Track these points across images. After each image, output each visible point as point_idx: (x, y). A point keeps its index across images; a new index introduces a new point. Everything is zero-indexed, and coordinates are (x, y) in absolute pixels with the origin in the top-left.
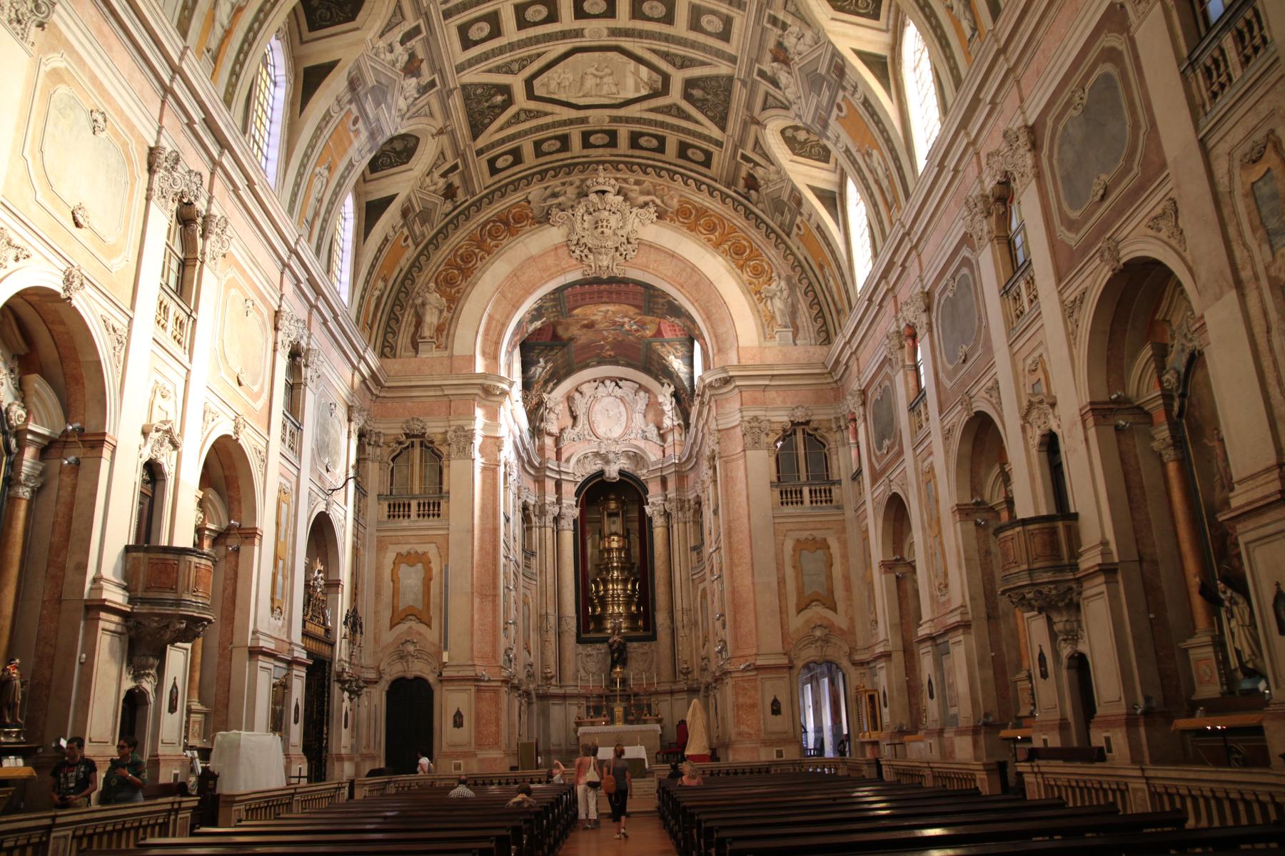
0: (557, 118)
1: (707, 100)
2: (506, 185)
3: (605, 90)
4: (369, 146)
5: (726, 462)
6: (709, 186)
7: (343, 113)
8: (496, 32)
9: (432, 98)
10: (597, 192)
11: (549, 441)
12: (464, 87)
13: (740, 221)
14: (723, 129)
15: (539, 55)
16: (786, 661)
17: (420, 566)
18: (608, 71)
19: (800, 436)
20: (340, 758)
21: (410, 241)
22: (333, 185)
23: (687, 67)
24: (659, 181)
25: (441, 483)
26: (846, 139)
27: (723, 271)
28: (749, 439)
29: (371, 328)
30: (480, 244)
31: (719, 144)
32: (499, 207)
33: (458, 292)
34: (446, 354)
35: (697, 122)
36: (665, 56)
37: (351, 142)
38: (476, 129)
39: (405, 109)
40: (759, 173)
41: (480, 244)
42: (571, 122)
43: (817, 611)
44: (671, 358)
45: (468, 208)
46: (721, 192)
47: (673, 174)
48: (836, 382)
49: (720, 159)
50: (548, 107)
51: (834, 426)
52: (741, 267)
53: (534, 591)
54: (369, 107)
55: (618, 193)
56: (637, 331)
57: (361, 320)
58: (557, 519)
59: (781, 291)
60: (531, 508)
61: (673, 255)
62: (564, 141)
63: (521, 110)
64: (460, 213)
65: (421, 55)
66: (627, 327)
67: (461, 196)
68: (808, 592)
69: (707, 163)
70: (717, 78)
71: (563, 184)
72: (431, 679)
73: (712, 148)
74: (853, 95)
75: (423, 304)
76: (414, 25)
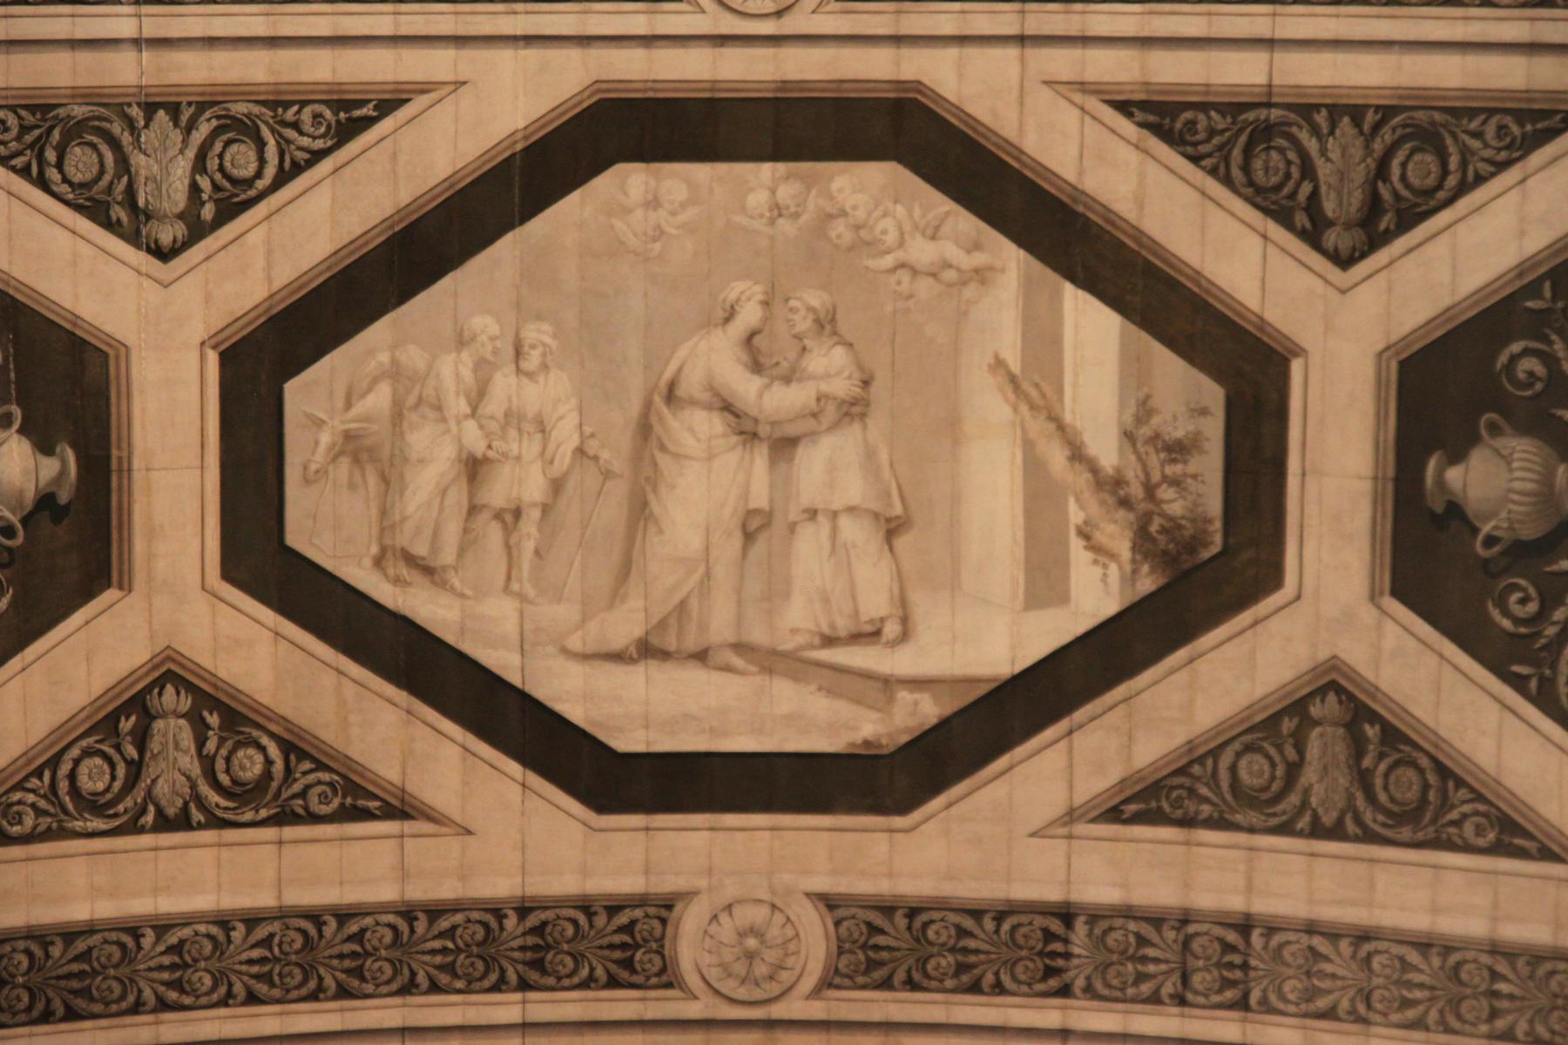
18: (830, 367)
50: (377, 725)
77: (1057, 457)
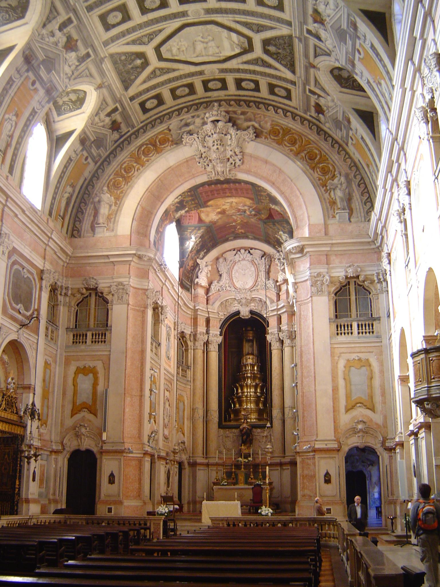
0: (182, 73)
1: (279, 53)
2: (156, 119)
3: (211, 51)
4: (47, 99)
5: (300, 305)
6: (292, 113)
7: (22, 79)
8: (127, 17)
9: (89, 64)
10: (213, 122)
11: (201, 292)
12: (112, 56)
13: (313, 136)
14: (294, 72)
15: (160, 31)
16: (336, 446)
17: (91, 375)
19: (352, 287)
20: (27, 501)
21: (89, 160)
22: (21, 125)
23: (261, 31)
24: (259, 111)
25: (107, 321)
26: (367, 75)
27: (300, 171)
28: (314, 289)
29: (63, 218)
30: (138, 160)
31: (293, 83)
32: (150, 134)
33: (122, 192)
34: (112, 234)
35: (276, 69)
36: (246, 25)
37: (32, 97)
38: (127, 84)
39: (71, 73)
40: (322, 102)
41: (138, 160)
42: (192, 75)
43: (360, 412)
44: (281, 233)
45: (130, 136)
46: (301, 117)
47: (267, 106)
48: (378, 248)
49: (295, 93)
51: (376, 279)
52: (313, 169)
53: (188, 393)
54: (43, 73)
55: (230, 120)
56: (255, 215)
57: (54, 213)
58: (207, 344)
59: (341, 184)
60: (188, 337)
61: (266, 162)
62: (191, 87)
63: (156, 68)
64: (125, 140)
65: (75, 36)
66: (248, 212)
67: (124, 128)
68: (354, 397)
69: (289, 97)
70: (282, 37)
71: (193, 117)
72: (95, 450)
73: (289, 86)
74: (364, 42)
75: (99, 202)
76: (66, 17)
77: (232, 43)
